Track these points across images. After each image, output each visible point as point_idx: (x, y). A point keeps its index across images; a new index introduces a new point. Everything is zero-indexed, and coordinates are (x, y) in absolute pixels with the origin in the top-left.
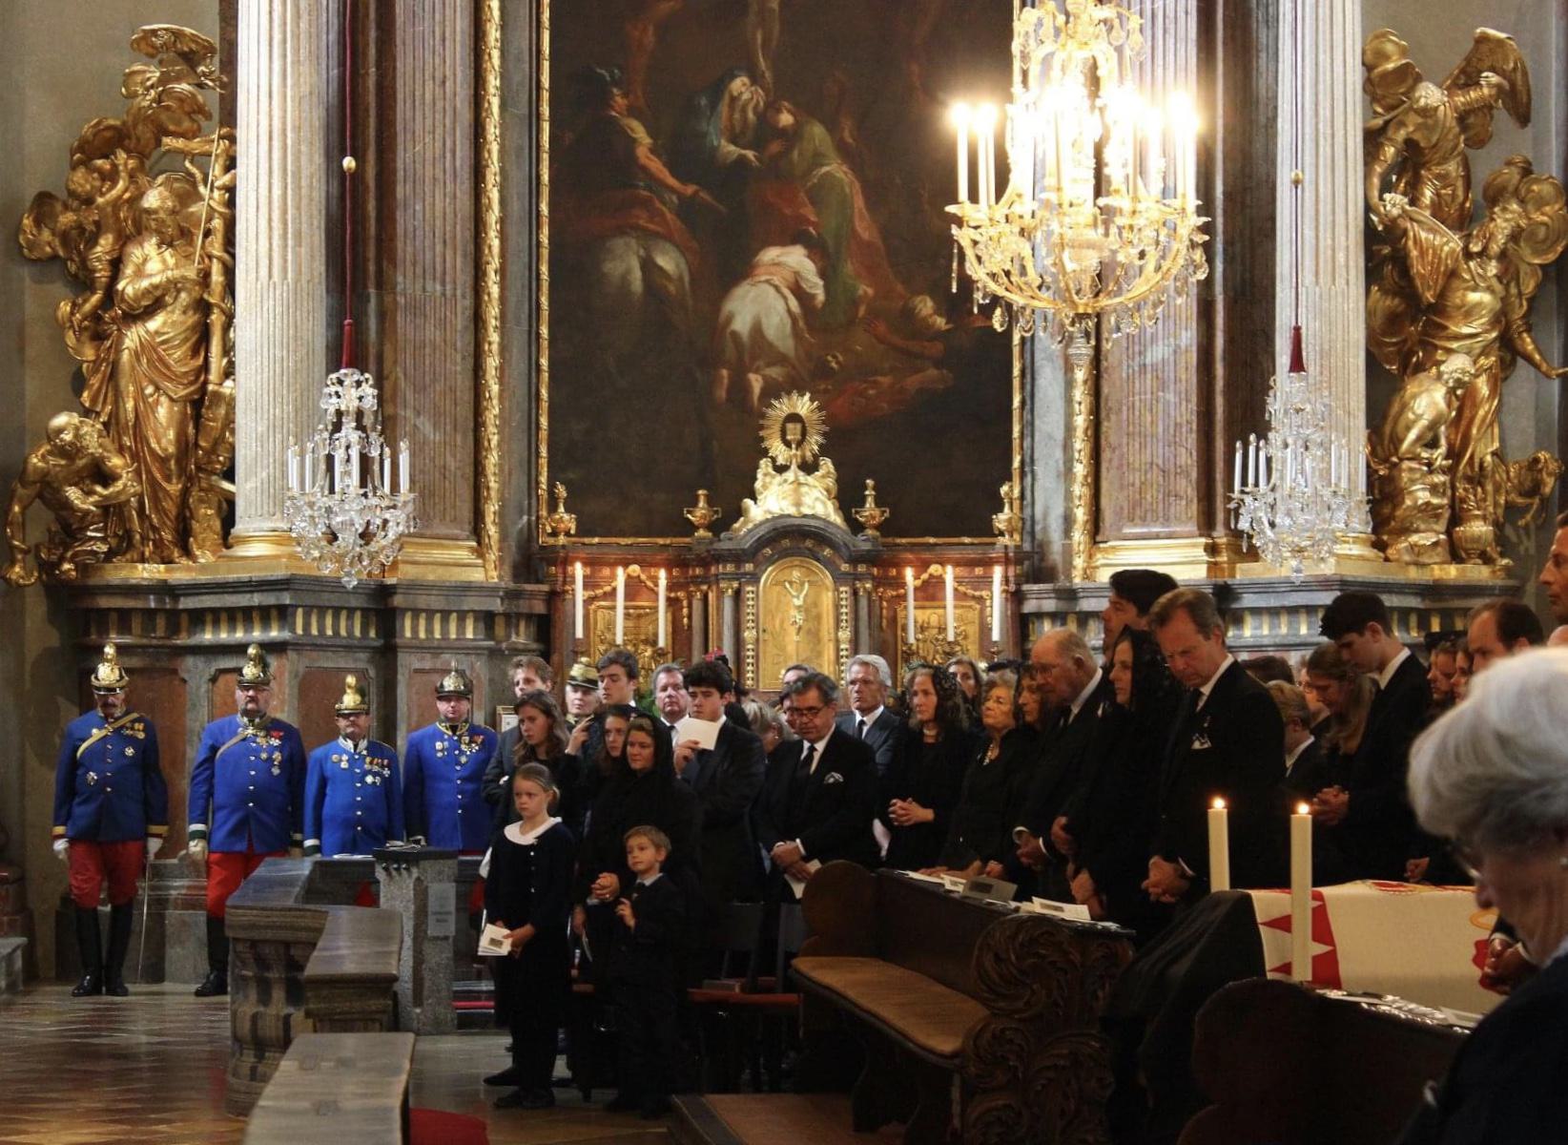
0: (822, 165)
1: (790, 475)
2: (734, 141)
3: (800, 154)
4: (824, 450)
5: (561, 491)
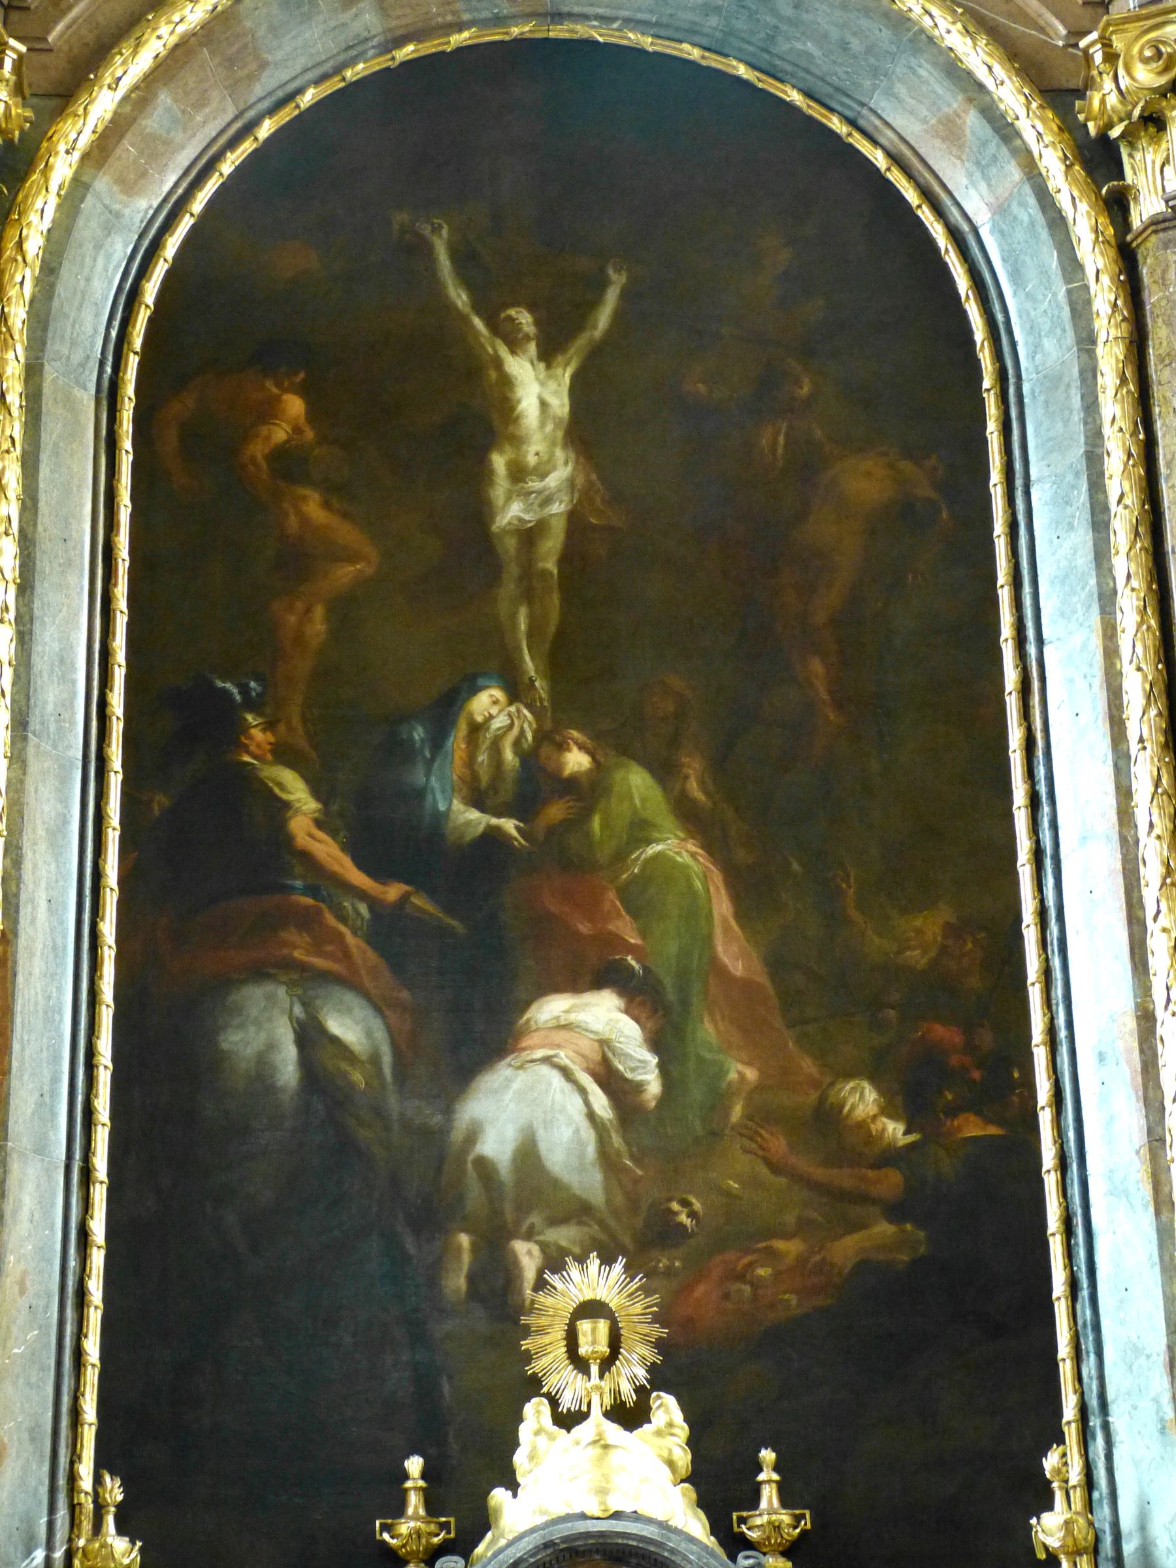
0: (649, 842)
1: (583, 1431)
2: (477, 800)
3: (605, 825)
4: (660, 1379)
5: (114, 1491)
